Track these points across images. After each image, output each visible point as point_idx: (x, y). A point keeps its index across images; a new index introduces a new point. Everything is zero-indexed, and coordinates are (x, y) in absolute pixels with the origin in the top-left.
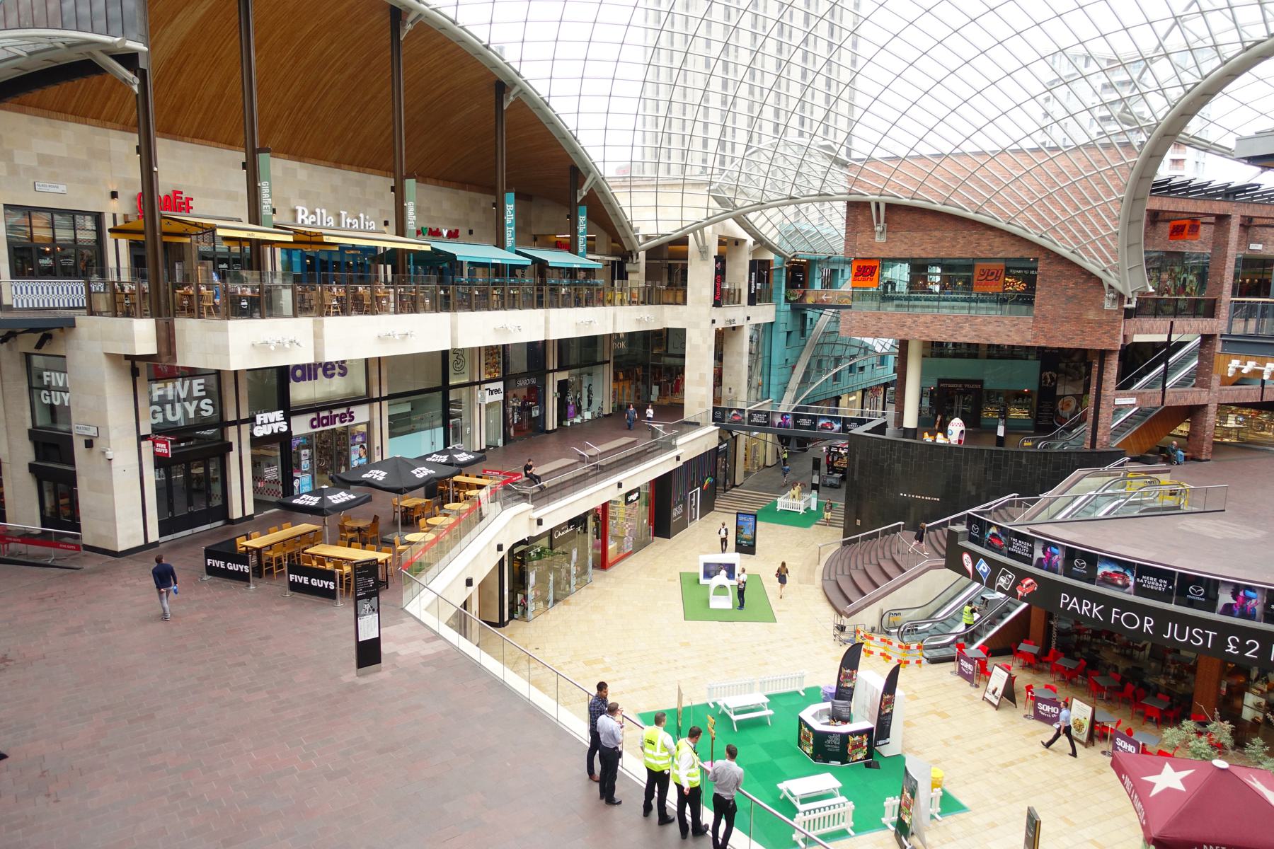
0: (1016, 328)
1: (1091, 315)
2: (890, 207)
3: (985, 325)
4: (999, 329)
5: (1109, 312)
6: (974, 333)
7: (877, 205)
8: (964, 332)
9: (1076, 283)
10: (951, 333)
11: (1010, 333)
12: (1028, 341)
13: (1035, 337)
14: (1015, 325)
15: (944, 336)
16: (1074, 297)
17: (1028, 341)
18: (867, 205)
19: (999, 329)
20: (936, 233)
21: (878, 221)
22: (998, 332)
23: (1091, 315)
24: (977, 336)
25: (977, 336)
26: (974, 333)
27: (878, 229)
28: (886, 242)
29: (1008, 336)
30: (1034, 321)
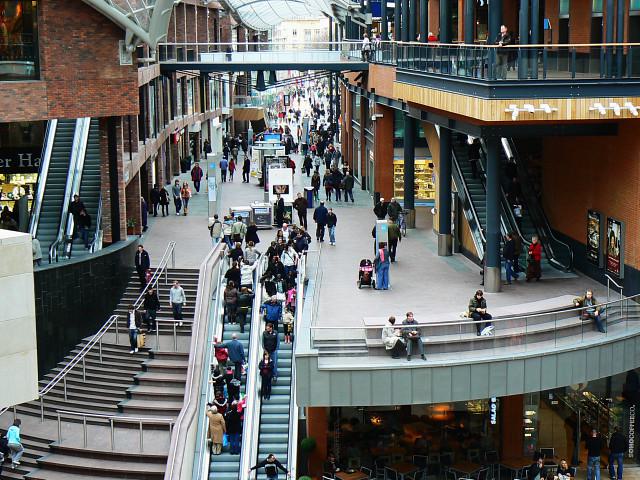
1: (108, 74)
4: (7, 101)
9: (88, 34)
11: (20, 106)
14: (27, 94)
16: (88, 52)
19: (7, 101)
22: (7, 105)
23: (108, 74)
29: (20, 109)
30: (48, 87)
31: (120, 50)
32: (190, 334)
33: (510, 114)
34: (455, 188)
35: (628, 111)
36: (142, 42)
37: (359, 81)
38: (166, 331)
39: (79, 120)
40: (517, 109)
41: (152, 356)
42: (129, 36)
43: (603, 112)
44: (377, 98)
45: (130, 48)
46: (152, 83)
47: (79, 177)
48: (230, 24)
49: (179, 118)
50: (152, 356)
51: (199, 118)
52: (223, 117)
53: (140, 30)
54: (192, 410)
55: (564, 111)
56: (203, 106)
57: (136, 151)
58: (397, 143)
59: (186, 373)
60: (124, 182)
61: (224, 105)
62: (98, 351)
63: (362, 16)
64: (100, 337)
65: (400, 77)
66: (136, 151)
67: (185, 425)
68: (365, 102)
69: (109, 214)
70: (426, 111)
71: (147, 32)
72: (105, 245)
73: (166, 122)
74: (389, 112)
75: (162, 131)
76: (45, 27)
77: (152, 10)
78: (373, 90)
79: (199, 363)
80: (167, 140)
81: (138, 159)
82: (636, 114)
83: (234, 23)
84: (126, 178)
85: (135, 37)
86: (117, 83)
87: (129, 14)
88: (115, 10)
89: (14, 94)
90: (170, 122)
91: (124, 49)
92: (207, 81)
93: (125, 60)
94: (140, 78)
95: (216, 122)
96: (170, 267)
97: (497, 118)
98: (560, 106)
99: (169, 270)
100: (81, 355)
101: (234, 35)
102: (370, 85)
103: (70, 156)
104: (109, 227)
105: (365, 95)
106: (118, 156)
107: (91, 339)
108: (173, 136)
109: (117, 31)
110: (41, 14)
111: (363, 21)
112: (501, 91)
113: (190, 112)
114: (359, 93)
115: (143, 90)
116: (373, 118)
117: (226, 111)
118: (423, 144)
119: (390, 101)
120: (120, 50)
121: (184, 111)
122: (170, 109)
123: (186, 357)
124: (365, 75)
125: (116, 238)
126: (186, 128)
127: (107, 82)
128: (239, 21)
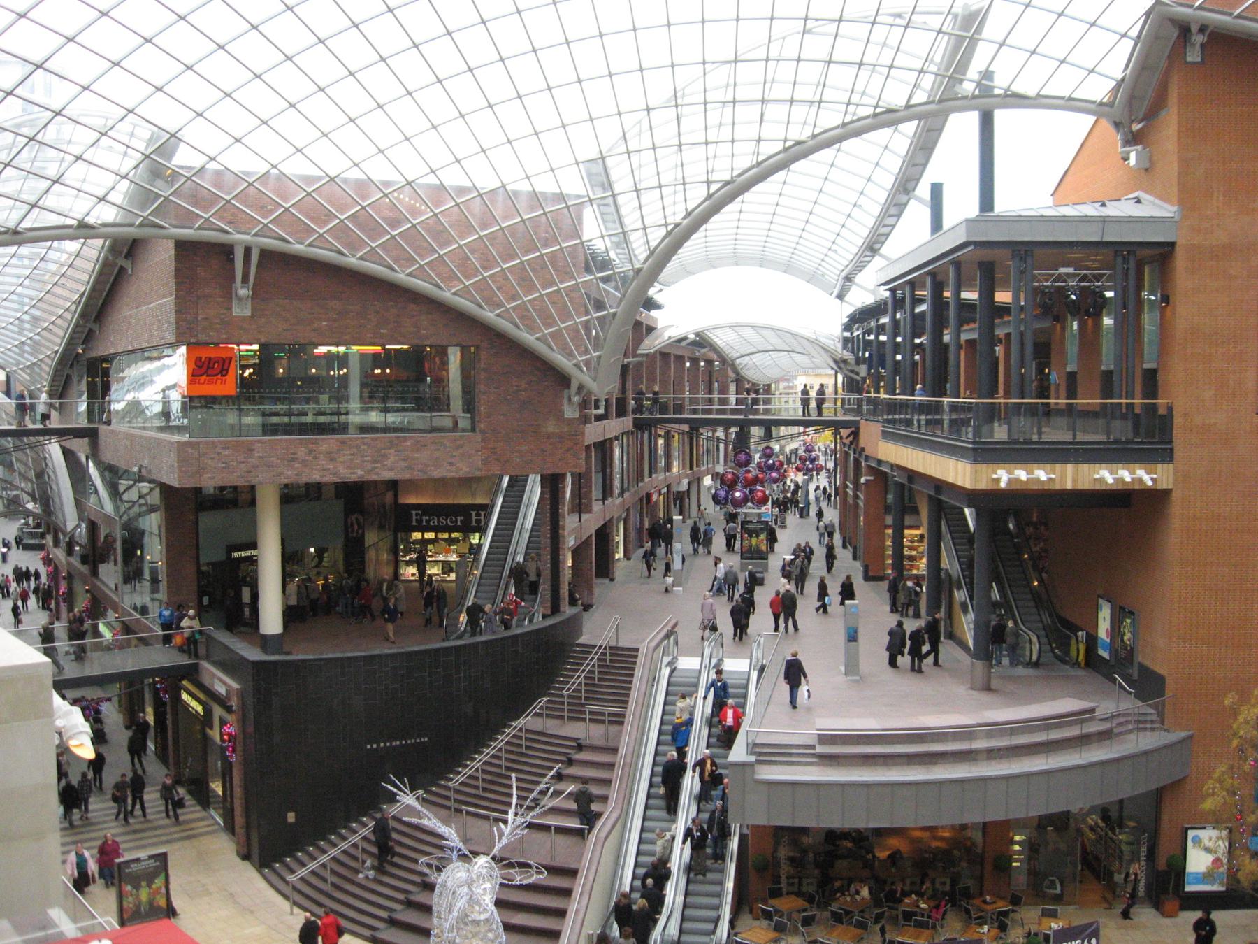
0: (461, 451)
1: (551, 427)
2: (267, 256)
3: (418, 451)
4: (437, 454)
5: (570, 421)
6: (403, 464)
7: (248, 250)
8: (389, 462)
9: (529, 383)
10: (369, 466)
12: (480, 470)
13: (486, 462)
14: (458, 448)
15: (360, 473)
17: (480, 470)
18: (226, 251)
19: (437, 454)
20: (335, 304)
21: (245, 280)
23: (551, 427)
24: (409, 467)
25: (409, 467)
26: (403, 464)
27: (244, 292)
28: (253, 316)
29: (451, 464)
30: (483, 440)
31: (565, 401)
32: (622, 723)
33: (998, 480)
34: (945, 563)
35: (1141, 480)
36: (589, 393)
37: (851, 438)
38: (597, 719)
39: (531, 477)
40: (1004, 476)
41: (580, 747)
42: (574, 386)
43: (1110, 481)
44: (867, 458)
45: (576, 399)
46: (617, 438)
47: (526, 536)
48: (727, 376)
49: (660, 477)
50: (580, 747)
51: (687, 476)
52: (716, 476)
53: (586, 379)
54: (615, 815)
55: (1063, 477)
56: (692, 462)
57: (590, 511)
58: (887, 509)
59: (613, 770)
60: (566, 546)
61: (718, 463)
62: (520, 738)
63: (856, 369)
64: (521, 722)
65: (886, 435)
66: (590, 511)
67: (603, 835)
68: (857, 462)
69: (549, 583)
70: (912, 475)
71: (595, 381)
72: (544, 617)
73: (639, 477)
74: (882, 475)
75: (633, 490)
76: (483, 375)
77: (599, 357)
78: (863, 449)
79: (628, 760)
80: (641, 499)
81: (592, 522)
82: (1150, 483)
83: (732, 375)
84: (571, 542)
85: (581, 388)
86: (561, 437)
87: (574, 362)
88: (559, 356)
89: (445, 447)
90: (647, 479)
91: (570, 400)
92: (698, 438)
93: (570, 412)
94: (587, 434)
95: (707, 481)
96: (613, 643)
97: (983, 485)
98: (1058, 473)
99: (611, 648)
100: (501, 740)
101: (733, 387)
102: (862, 444)
103: (517, 513)
104: (548, 597)
105: (857, 456)
106: (561, 518)
107: (514, 724)
108: (649, 496)
109: (563, 380)
110: (479, 361)
111: (858, 374)
112: (985, 453)
113: (675, 470)
114: (851, 452)
115: (588, 447)
116: (862, 480)
117: (720, 469)
118: (915, 511)
119: (880, 462)
120: (565, 401)
121: (668, 467)
122: (642, 465)
123: (615, 750)
124: (855, 434)
125: (555, 609)
126: (668, 487)
127: (549, 436)
128: (738, 373)
